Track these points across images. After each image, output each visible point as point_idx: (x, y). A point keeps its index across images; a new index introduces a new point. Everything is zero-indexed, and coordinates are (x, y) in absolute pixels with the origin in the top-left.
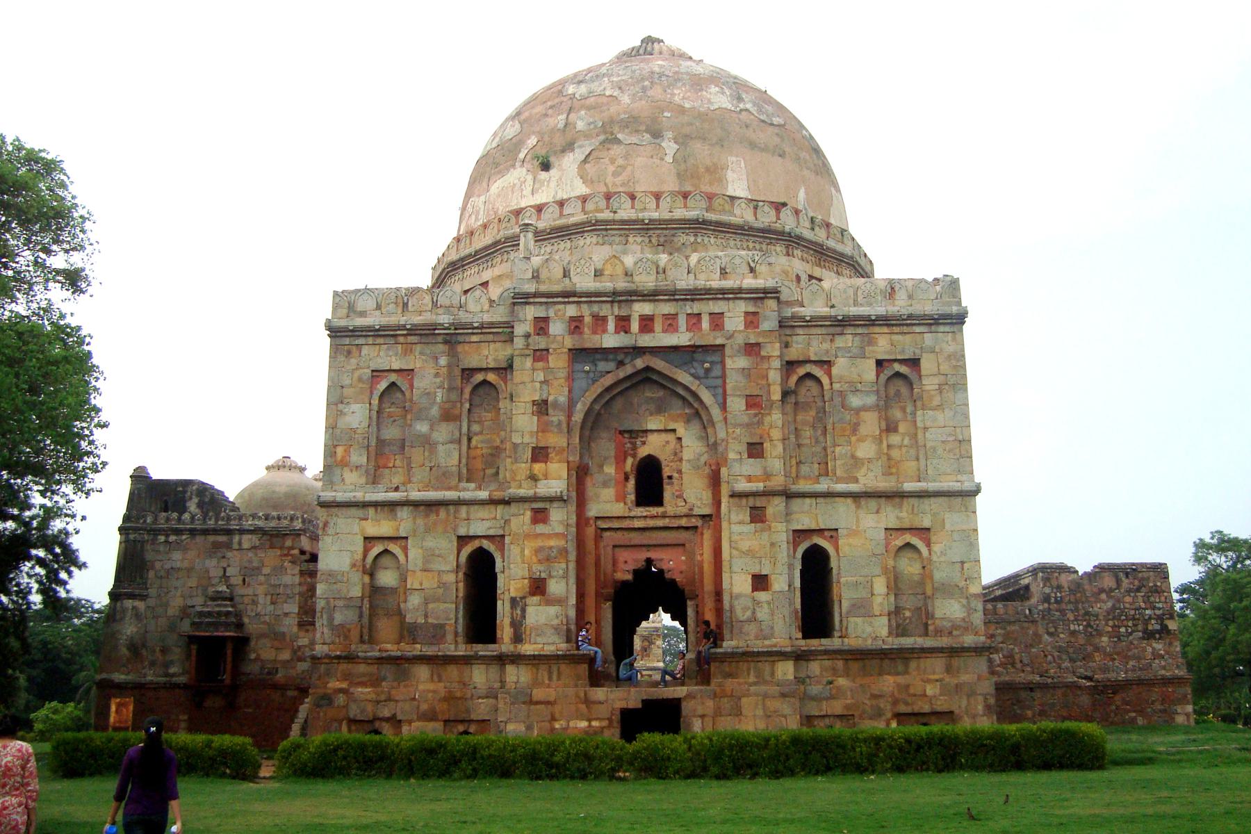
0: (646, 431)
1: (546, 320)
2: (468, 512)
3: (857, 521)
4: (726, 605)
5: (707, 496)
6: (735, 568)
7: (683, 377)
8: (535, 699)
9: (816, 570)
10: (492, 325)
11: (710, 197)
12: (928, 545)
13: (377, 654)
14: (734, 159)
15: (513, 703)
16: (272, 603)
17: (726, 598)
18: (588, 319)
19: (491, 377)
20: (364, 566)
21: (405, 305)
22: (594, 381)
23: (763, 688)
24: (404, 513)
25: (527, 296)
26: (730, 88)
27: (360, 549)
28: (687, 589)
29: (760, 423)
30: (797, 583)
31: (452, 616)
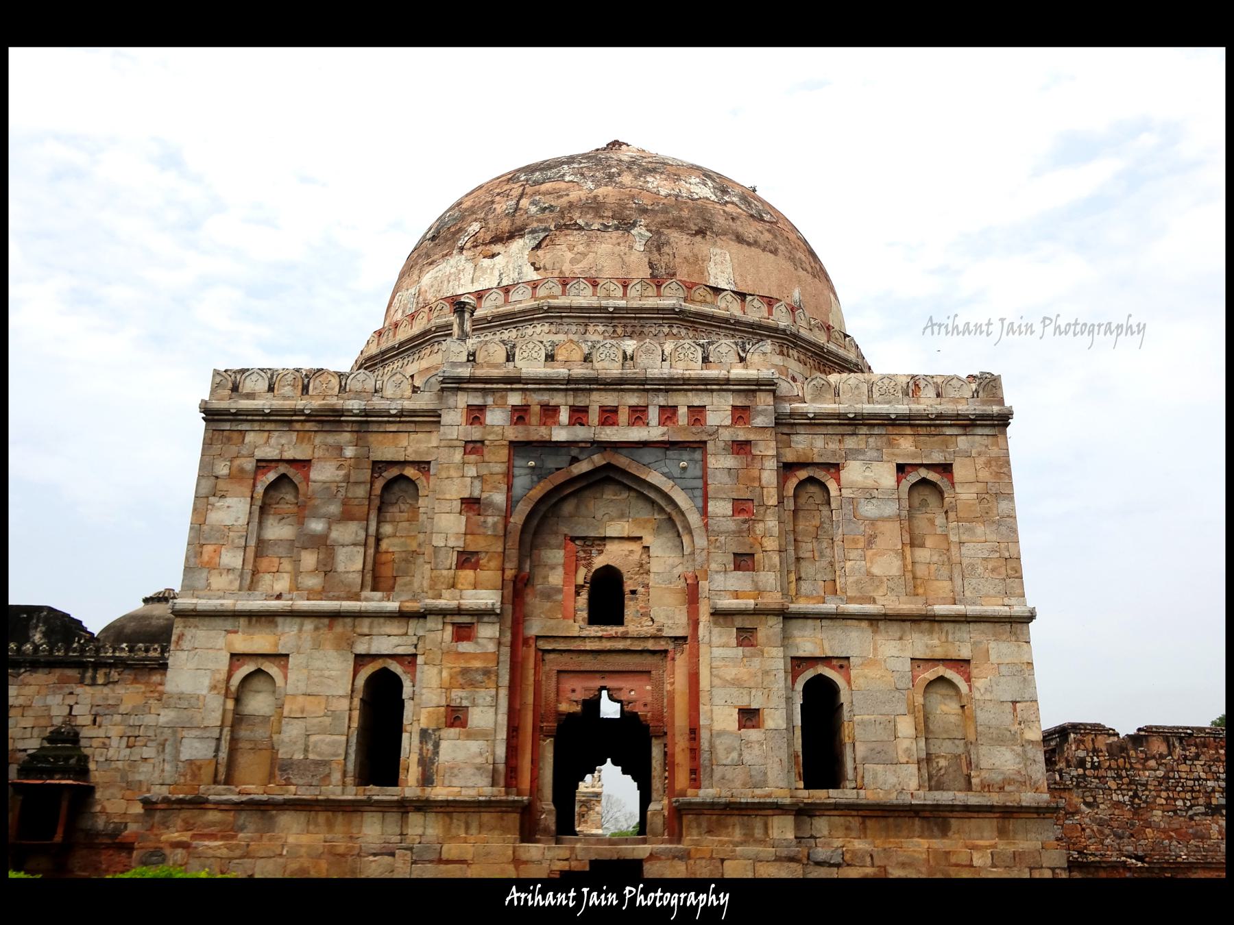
0: (605, 538)
1: (482, 408)
3: (875, 649)
4: (705, 744)
6: (716, 700)
8: (445, 856)
9: (821, 707)
10: (414, 413)
15: (414, 862)
17: (704, 735)
19: (410, 472)
20: (227, 688)
23: (752, 849)
25: (459, 380)
30: (798, 721)
31: (342, 751)
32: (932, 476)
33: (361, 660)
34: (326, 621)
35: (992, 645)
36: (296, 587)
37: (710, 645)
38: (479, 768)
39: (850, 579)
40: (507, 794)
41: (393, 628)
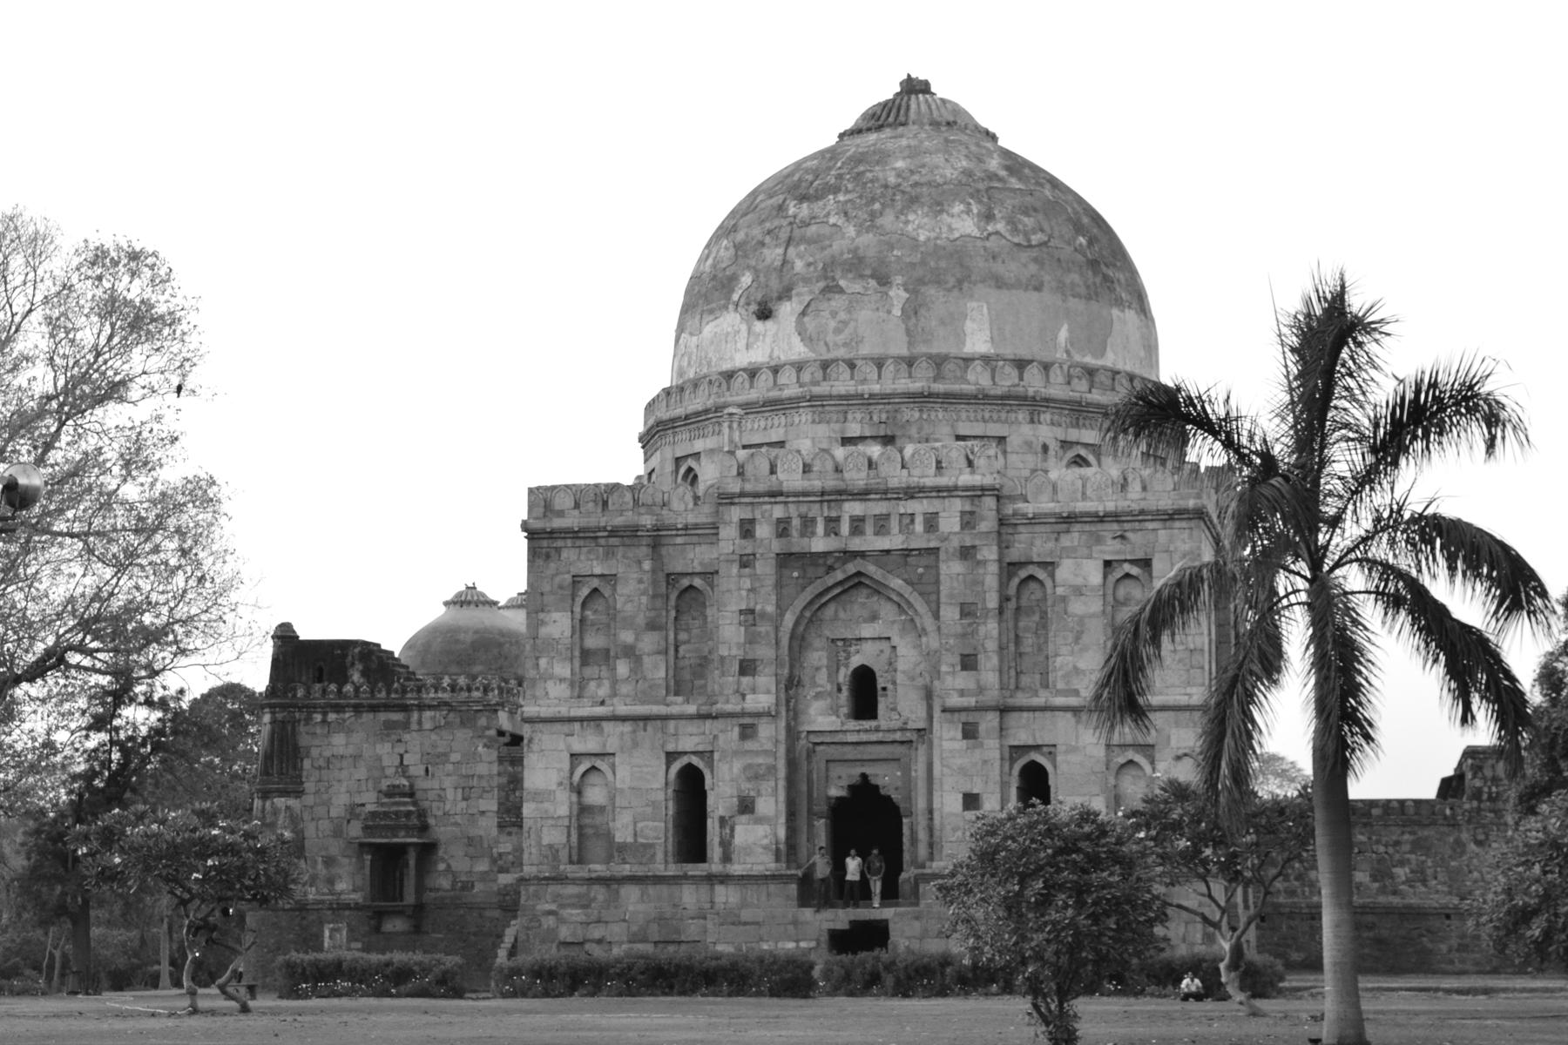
1: (752, 521)
2: (676, 728)
5: (922, 712)
6: (946, 787)
7: (896, 583)
10: (696, 526)
11: (939, 361)
12: (1152, 763)
13: (586, 875)
14: (974, 304)
16: (464, 799)
17: (936, 816)
18: (796, 522)
19: (697, 582)
21: (605, 503)
22: (804, 588)
24: (608, 727)
26: (980, 202)
27: (566, 765)
28: (902, 806)
29: (974, 633)
31: (662, 835)
32: (1135, 571)
33: (671, 757)
34: (641, 724)
35: (1174, 731)
36: (614, 694)
37: (941, 738)
38: (765, 848)
39: (1060, 673)
40: (788, 868)
41: (692, 727)
